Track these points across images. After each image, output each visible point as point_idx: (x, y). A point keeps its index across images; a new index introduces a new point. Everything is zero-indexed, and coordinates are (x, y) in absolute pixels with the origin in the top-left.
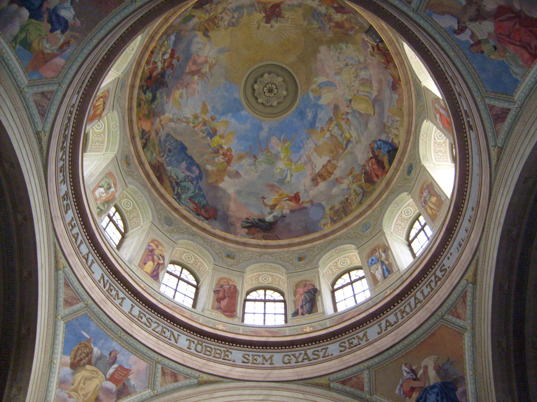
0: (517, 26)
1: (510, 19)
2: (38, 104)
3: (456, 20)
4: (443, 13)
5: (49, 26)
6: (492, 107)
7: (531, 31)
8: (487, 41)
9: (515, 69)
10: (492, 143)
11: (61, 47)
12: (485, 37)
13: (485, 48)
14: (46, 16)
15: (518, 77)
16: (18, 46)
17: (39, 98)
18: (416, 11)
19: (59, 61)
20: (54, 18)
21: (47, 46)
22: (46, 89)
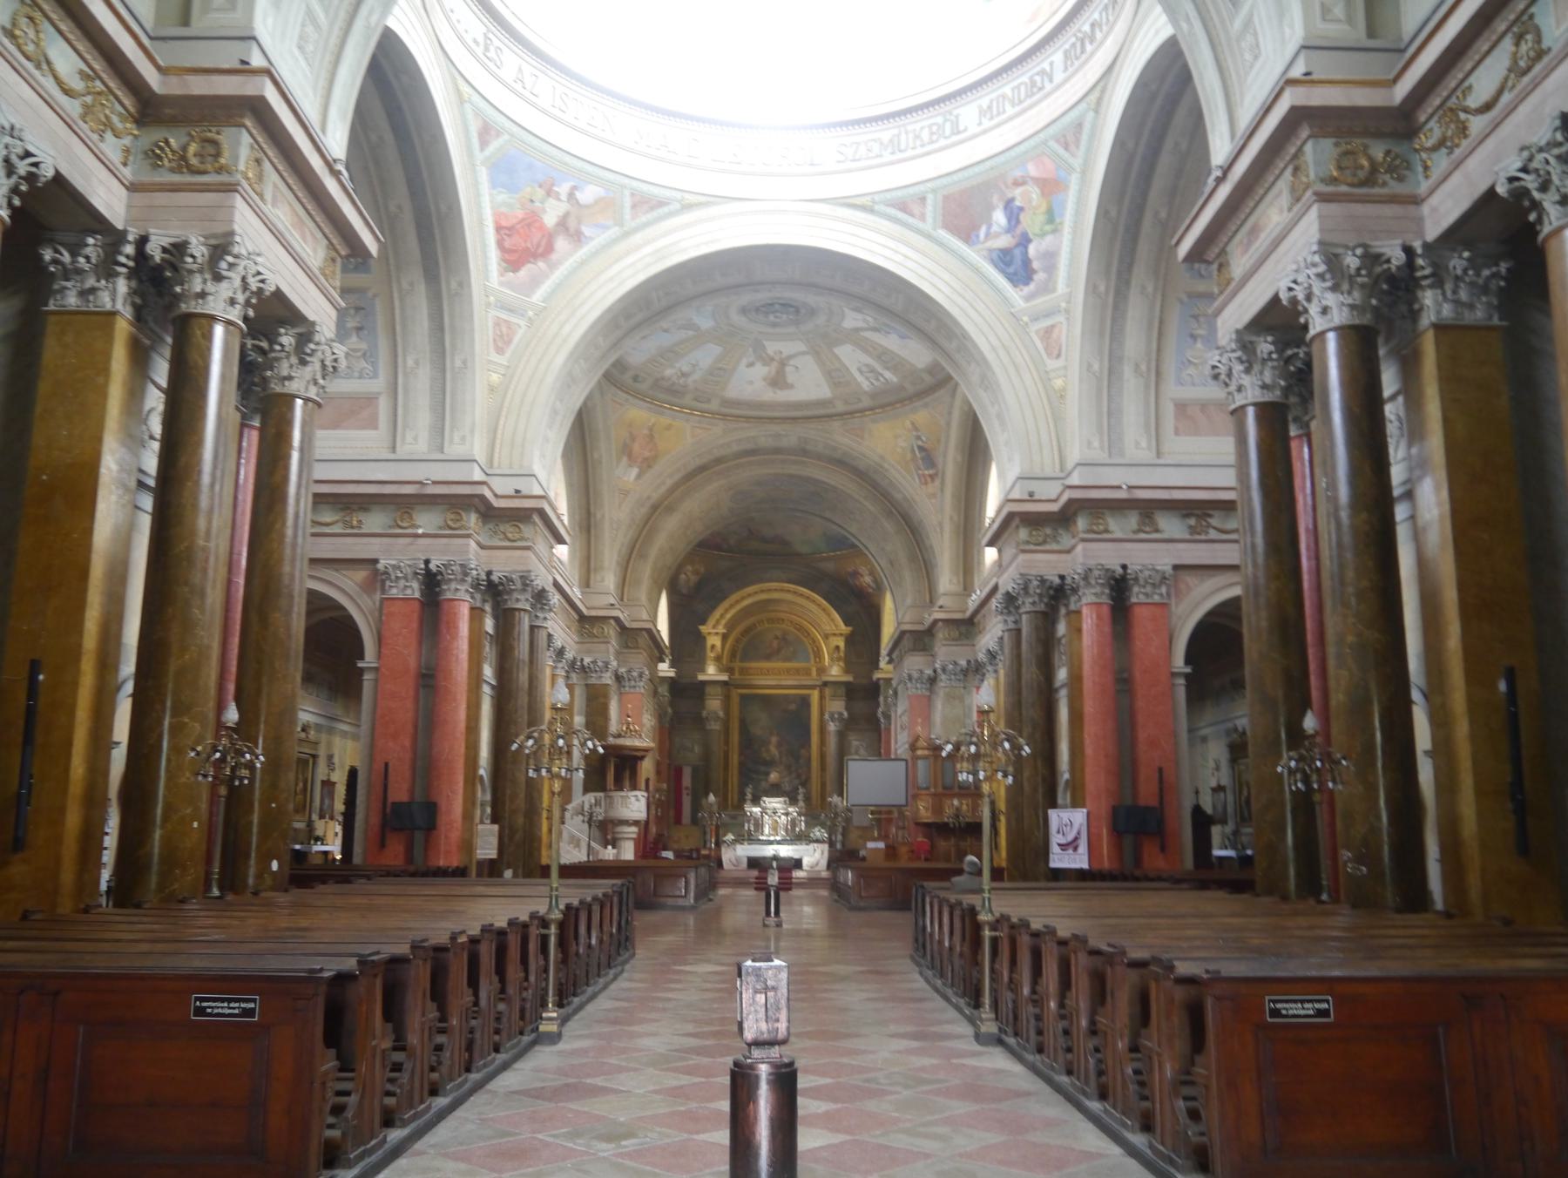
0: (529, 245)
1: (539, 245)
2: (1077, 142)
3: (581, 202)
4: (598, 201)
5: (1022, 217)
6: (498, 134)
7: (515, 251)
8: (542, 203)
9: (502, 197)
10: (476, 98)
11: (1023, 183)
12: (547, 205)
13: (540, 193)
14: (1018, 231)
15: (495, 192)
16: (1058, 220)
17: (1072, 147)
18: (623, 186)
19: (1032, 170)
20: (1013, 223)
21: (1034, 196)
22: (1061, 151)
